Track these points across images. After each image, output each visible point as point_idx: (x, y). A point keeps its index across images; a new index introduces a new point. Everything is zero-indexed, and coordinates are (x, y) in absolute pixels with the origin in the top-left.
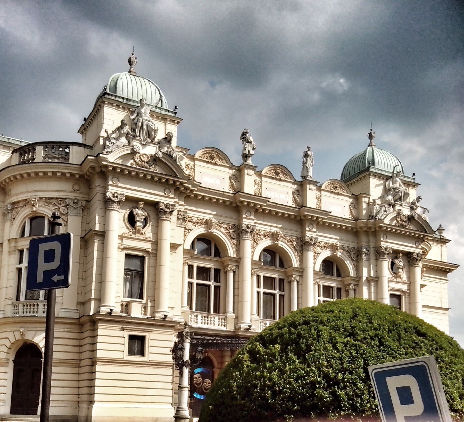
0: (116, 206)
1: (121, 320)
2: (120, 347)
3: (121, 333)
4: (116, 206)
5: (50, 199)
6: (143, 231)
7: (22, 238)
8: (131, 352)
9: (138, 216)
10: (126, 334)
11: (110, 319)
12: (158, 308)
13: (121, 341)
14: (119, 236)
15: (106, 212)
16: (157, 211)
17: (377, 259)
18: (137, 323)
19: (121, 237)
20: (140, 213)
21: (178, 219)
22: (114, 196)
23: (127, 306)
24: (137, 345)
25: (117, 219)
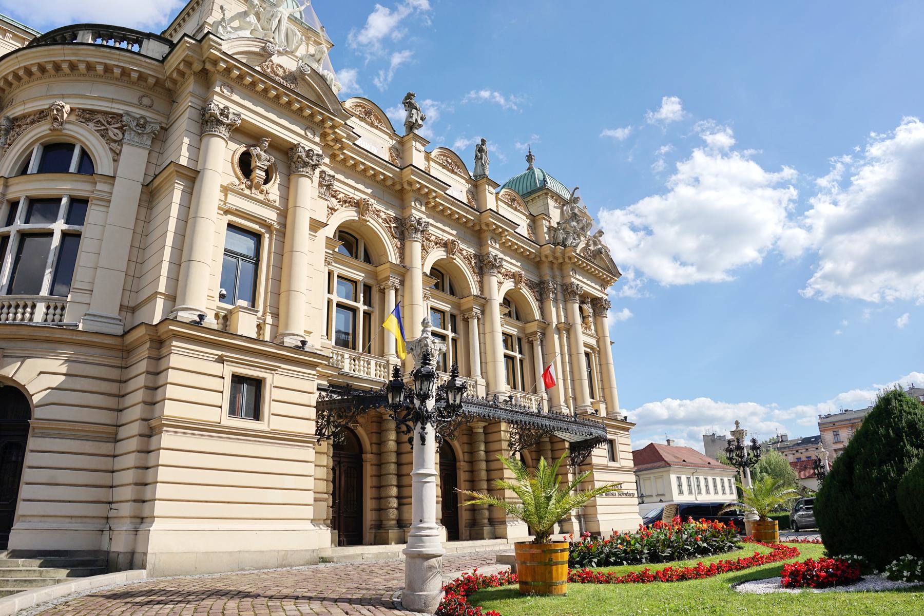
0: (223, 130)
1: (219, 338)
2: (215, 398)
3: (217, 368)
4: (223, 130)
5: (92, 112)
6: (265, 187)
7: (24, 177)
8: (233, 412)
9: (259, 159)
10: (228, 370)
11: (197, 334)
12: (287, 326)
13: (216, 384)
14: (222, 186)
15: (201, 140)
16: (289, 160)
17: (565, 301)
18: (249, 349)
19: (225, 190)
20: (262, 158)
21: (321, 185)
22: (221, 114)
23: (225, 318)
24: (249, 395)
25: (222, 154)
